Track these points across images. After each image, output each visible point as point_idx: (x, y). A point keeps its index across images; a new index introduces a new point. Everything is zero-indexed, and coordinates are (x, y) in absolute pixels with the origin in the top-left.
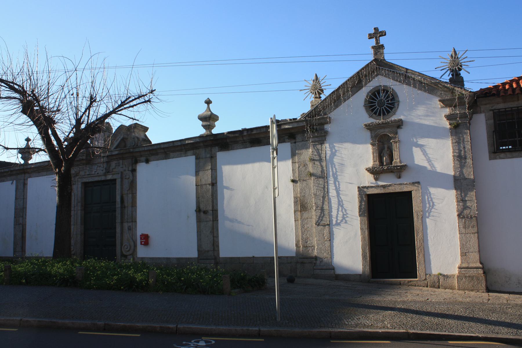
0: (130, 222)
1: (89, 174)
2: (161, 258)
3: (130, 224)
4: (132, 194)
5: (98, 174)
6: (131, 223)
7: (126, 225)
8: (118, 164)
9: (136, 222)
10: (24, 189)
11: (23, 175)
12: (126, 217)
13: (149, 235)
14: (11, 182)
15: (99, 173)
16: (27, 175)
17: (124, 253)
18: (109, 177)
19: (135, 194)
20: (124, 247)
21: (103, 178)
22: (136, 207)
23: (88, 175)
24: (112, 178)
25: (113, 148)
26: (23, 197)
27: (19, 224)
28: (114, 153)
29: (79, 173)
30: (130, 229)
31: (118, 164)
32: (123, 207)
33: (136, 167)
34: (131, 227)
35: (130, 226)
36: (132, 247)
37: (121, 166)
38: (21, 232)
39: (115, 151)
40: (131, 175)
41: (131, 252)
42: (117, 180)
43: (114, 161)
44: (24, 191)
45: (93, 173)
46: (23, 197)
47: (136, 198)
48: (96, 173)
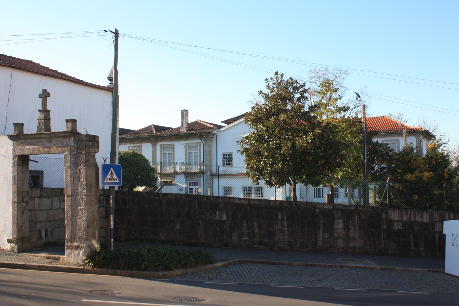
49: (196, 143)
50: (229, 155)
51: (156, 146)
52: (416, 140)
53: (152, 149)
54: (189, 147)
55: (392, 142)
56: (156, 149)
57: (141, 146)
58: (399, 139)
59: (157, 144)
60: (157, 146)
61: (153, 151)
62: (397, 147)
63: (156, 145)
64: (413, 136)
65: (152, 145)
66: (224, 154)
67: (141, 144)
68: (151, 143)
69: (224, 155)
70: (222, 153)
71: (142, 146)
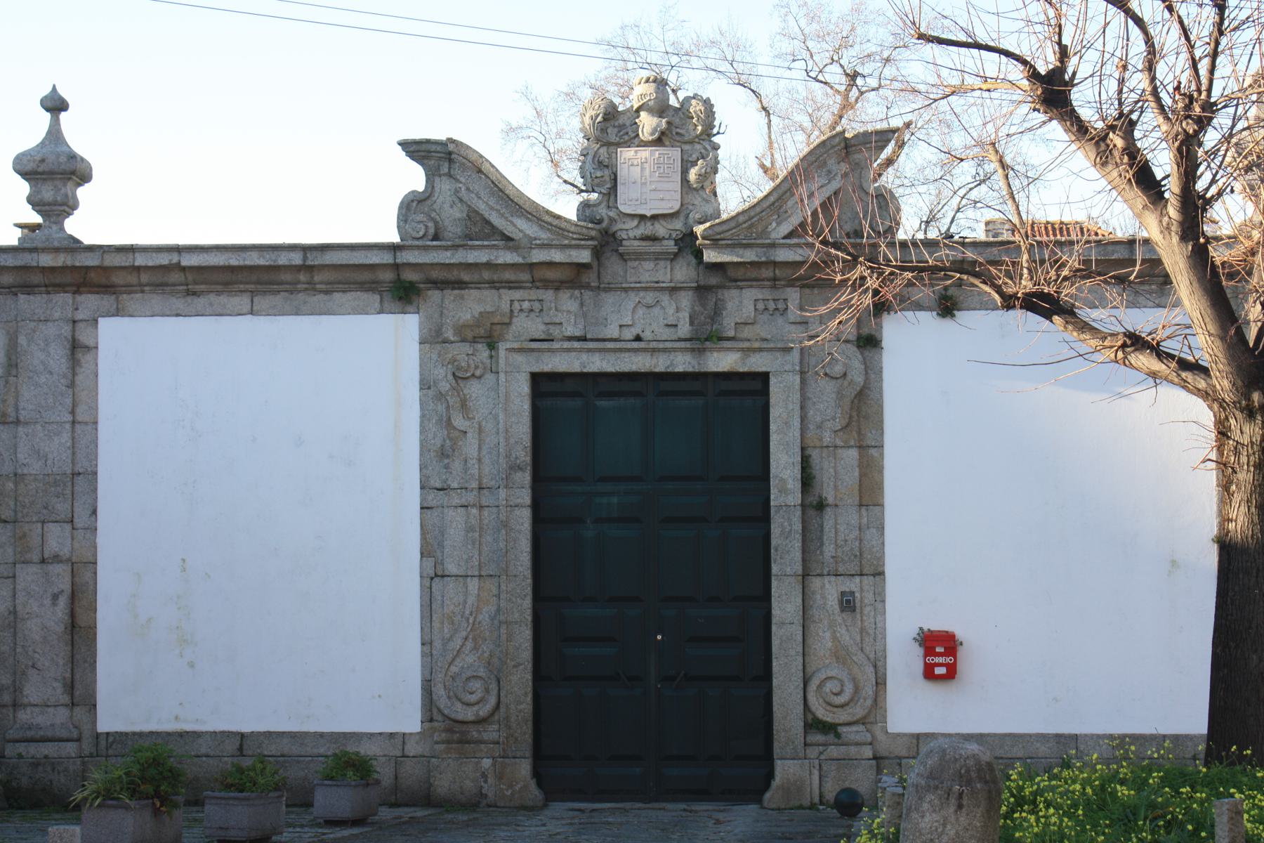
0: (853, 575)
1: (577, 334)
2: (1030, 735)
3: (852, 585)
4: (861, 448)
5: (638, 338)
6: (857, 579)
7: (828, 591)
8: (772, 306)
9: (879, 574)
10: (74, 374)
11: (68, 297)
12: (829, 550)
13: (960, 634)
15: (647, 335)
16: (89, 302)
17: (821, 713)
18: (722, 361)
19: (873, 452)
20: (820, 686)
21: (682, 363)
22: (882, 505)
23: (570, 339)
24: (742, 369)
25: (785, 228)
26: (70, 418)
27: (43, 561)
28: (783, 255)
29: (509, 324)
30: (848, 604)
31: (772, 306)
32: (814, 506)
33: (880, 326)
34: (857, 595)
35: (852, 593)
36: (869, 690)
37: (794, 312)
38: (63, 602)
39: (790, 246)
40: (857, 365)
41: (858, 711)
42: (773, 380)
43: (751, 287)
44: (72, 385)
45: (613, 331)
46: (70, 418)
47: (881, 470)
48: (628, 334)
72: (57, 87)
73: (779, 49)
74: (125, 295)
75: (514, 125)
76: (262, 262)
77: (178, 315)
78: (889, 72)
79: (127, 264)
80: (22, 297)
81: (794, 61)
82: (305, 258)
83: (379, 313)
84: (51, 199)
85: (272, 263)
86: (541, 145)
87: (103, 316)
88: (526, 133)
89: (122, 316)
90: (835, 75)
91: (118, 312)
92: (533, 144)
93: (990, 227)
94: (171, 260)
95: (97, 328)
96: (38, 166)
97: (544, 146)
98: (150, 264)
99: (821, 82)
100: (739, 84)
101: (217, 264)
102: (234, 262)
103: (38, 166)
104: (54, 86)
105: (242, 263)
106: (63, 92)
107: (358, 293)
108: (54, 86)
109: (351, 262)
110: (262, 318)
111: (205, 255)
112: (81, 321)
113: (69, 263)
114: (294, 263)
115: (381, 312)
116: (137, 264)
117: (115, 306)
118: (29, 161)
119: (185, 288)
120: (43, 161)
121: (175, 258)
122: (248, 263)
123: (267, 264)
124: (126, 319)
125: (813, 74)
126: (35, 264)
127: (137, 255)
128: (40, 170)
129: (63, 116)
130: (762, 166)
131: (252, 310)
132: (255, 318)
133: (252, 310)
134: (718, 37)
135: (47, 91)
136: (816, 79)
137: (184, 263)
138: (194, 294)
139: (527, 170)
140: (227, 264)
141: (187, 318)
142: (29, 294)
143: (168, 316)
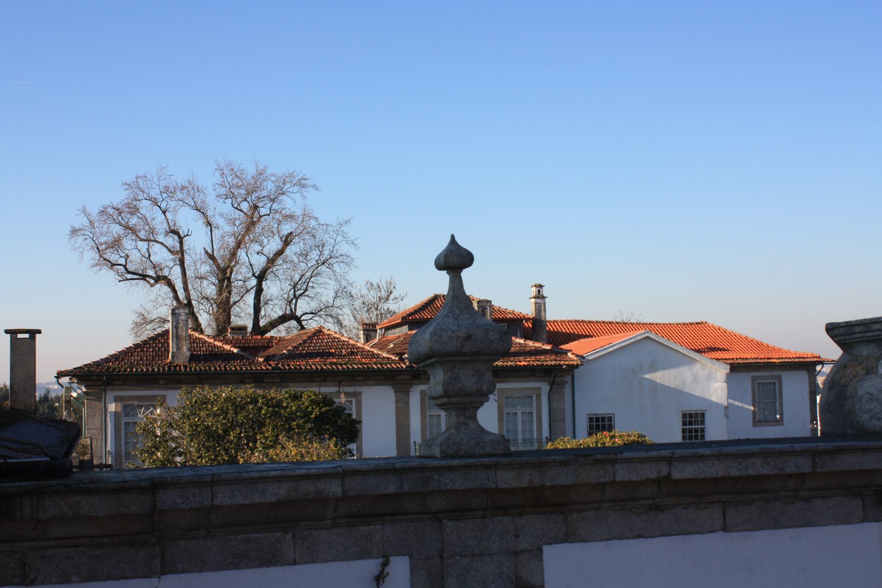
14: (371, 566)
49: (528, 389)
50: (603, 419)
51: (408, 396)
52: (809, 379)
53: (397, 402)
54: (506, 397)
55: (770, 381)
56: (407, 403)
57: (357, 395)
58: (781, 376)
59: (411, 390)
60: (411, 394)
61: (397, 407)
62: (777, 391)
63: (409, 391)
64: (804, 370)
65: (395, 392)
66: (590, 418)
67: (358, 389)
68: (393, 388)
69: (591, 420)
70: (588, 415)
71: (360, 393)
72: (457, 239)
73: (219, 192)
74: (575, 515)
75: (77, 228)
76: (766, 471)
77: (640, 536)
78: (275, 206)
79: (607, 480)
80: (449, 524)
81: (227, 198)
82: (814, 464)
83: (862, 521)
84: (474, 388)
85: (778, 472)
86: (91, 240)
87: (550, 544)
88: (83, 232)
89: (573, 542)
90: (245, 206)
91: (568, 537)
92: (86, 239)
93: (480, 304)
94: (659, 473)
95: (542, 560)
96: (463, 346)
97: (93, 240)
98: (635, 478)
99: (239, 210)
100: (197, 210)
101: (715, 476)
102: (734, 472)
103: (463, 346)
104: (453, 237)
105: (744, 473)
106: (462, 242)
107: (840, 498)
108: (453, 237)
109: (864, 468)
110: (735, 534)
111: (701, 465)
112: (522, 551)
113: (537, 482)
114: (802, 471)
115: (864, 520)
116: (618, 479)
117: (564, 530)
118: (451, 338)
119: (651, 502)
120: (468, 337)
121: (664, 469)
122: (751, 472)
123: (773, 473)
124: (577, 546)
125: (235, 206)
126: (493, 486)
127: (618, 467)
128: (466, 349)
129: (466, 274)
130: (207, 252)
131: (725, 526)
132: (727, 534)
133: (725, 526)
134: (187, 185)
135: (443, 244)
136: (236, 208)
137: (676, 475)
138: (658, 508)
139: (82, 252)
140: (726, 475)
141: (650, 540)
142: (458, 520)
143: (628, 538)
